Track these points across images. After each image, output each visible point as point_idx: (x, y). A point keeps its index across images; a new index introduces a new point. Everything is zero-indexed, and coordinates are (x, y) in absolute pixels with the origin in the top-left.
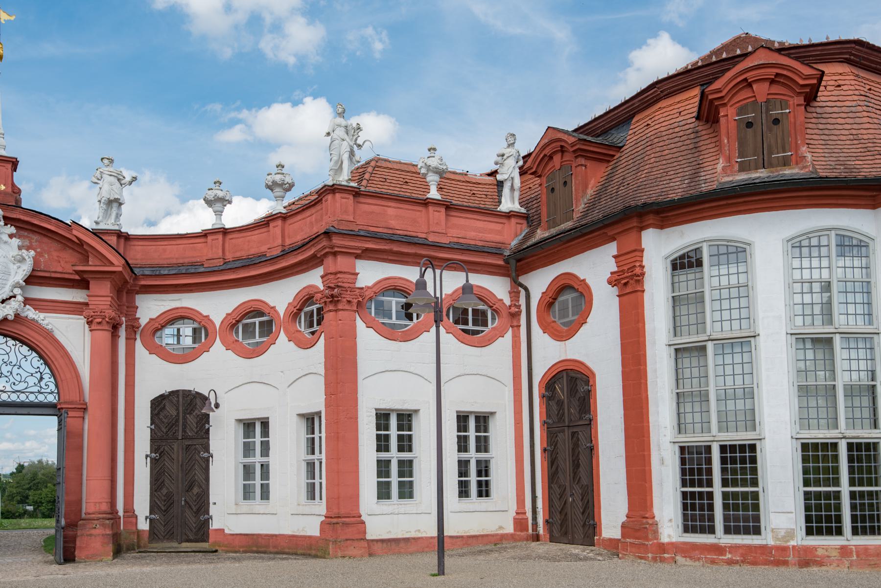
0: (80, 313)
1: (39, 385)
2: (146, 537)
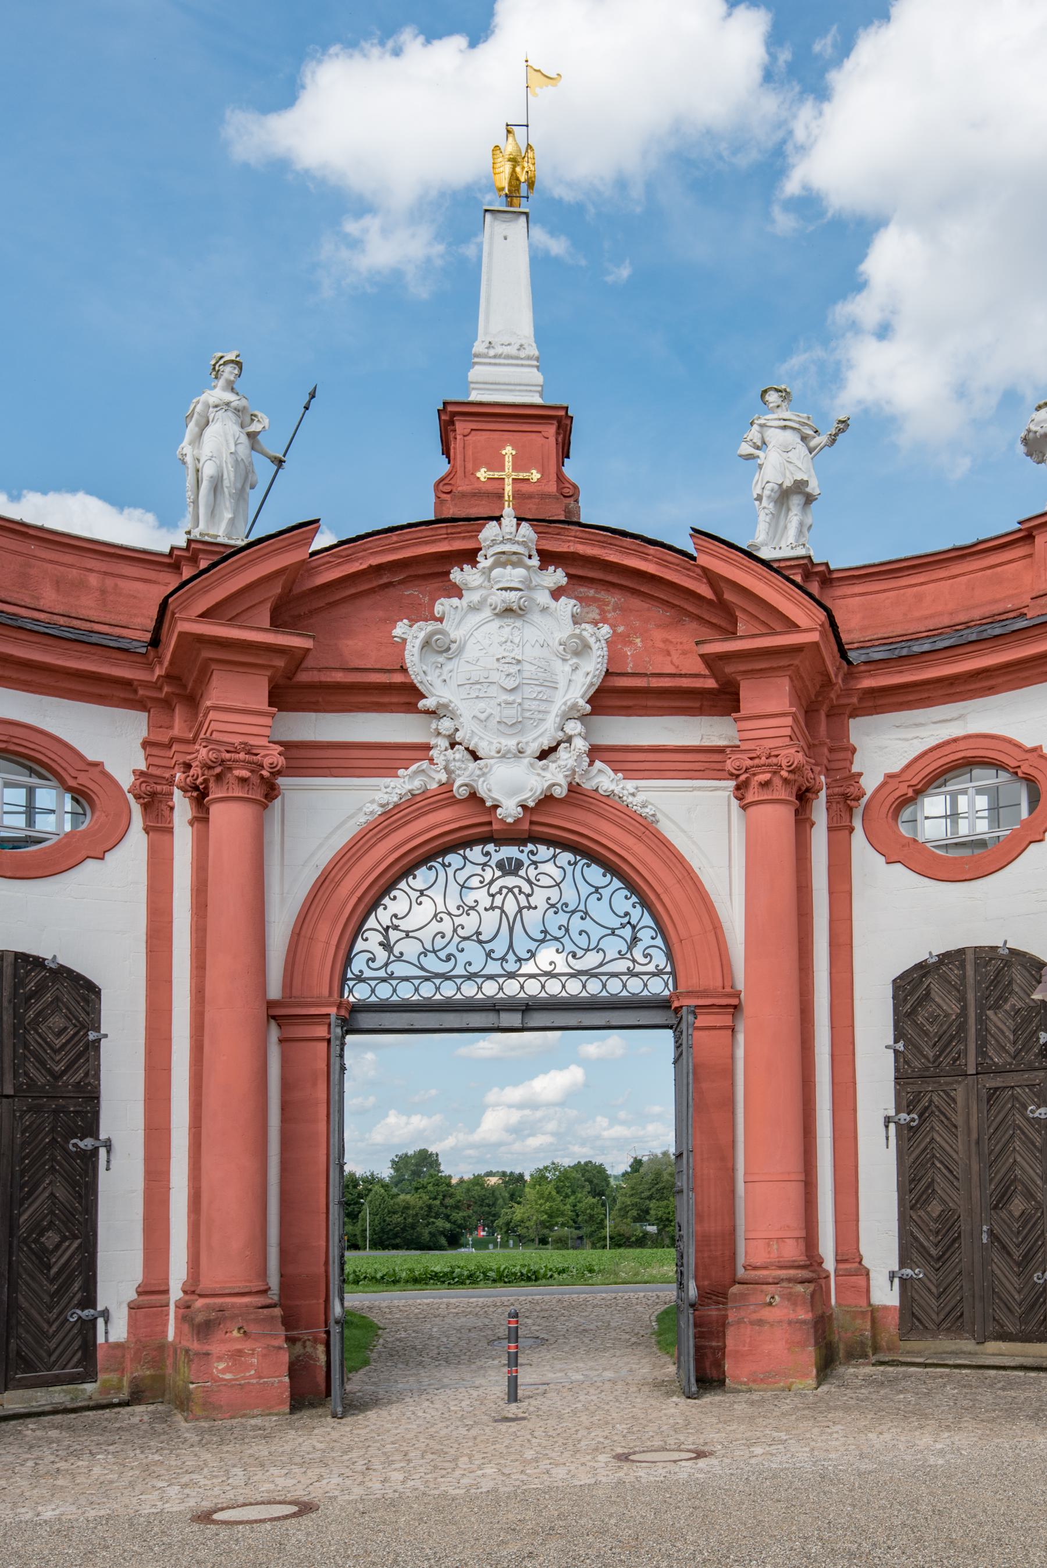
0: (717, 772)
1: (628, 956)
2: (892, 1324)
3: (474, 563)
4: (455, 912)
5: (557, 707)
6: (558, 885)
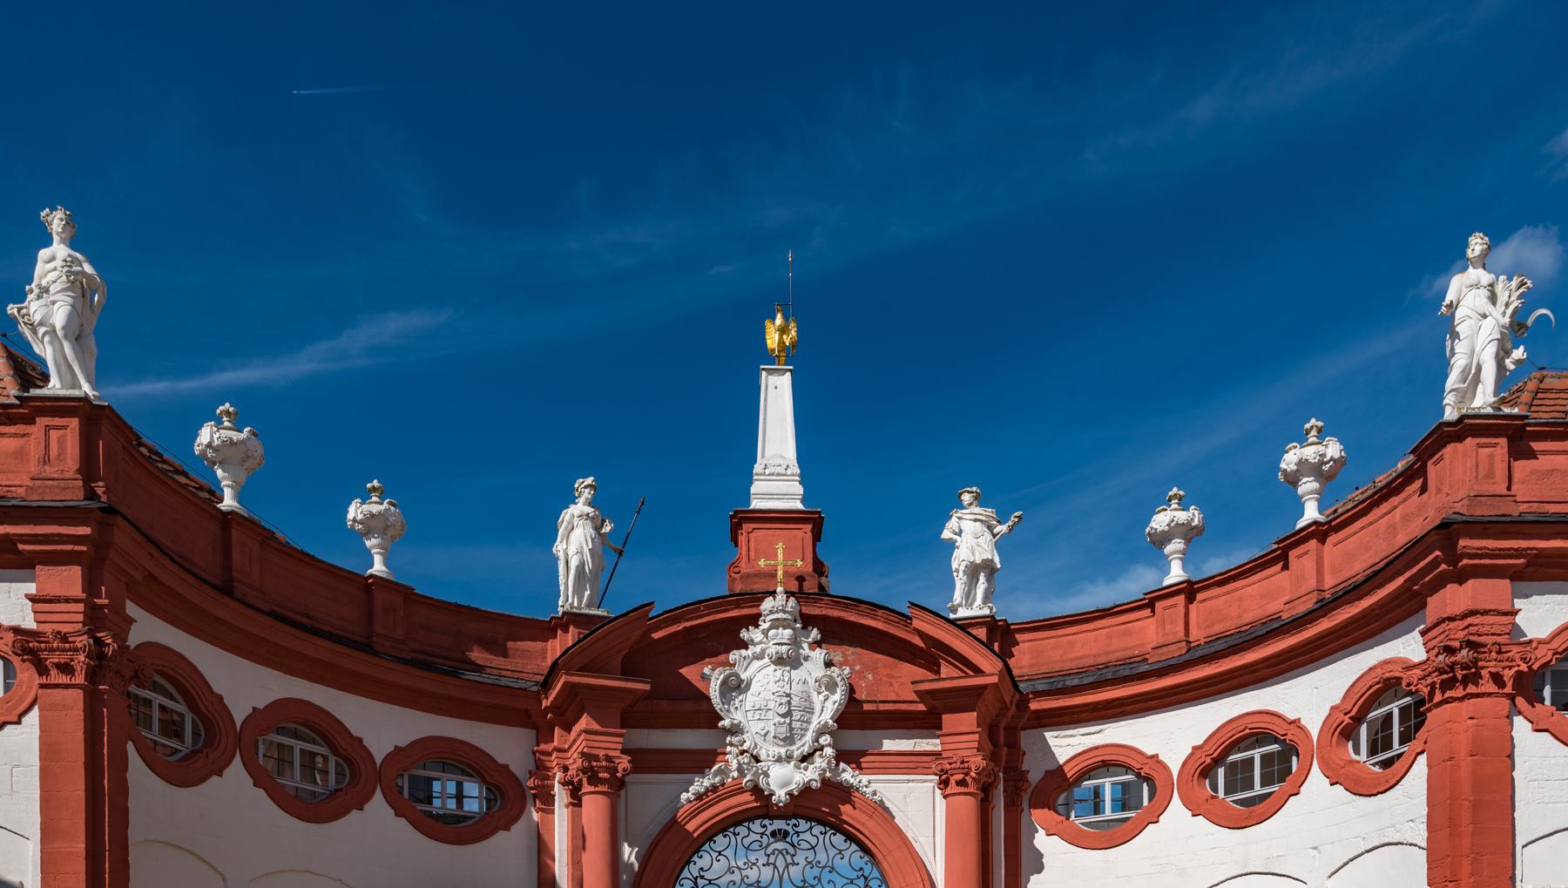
0: (925, 770)
3: (757, 626)
5: (813, 727)
6: (813, 848)
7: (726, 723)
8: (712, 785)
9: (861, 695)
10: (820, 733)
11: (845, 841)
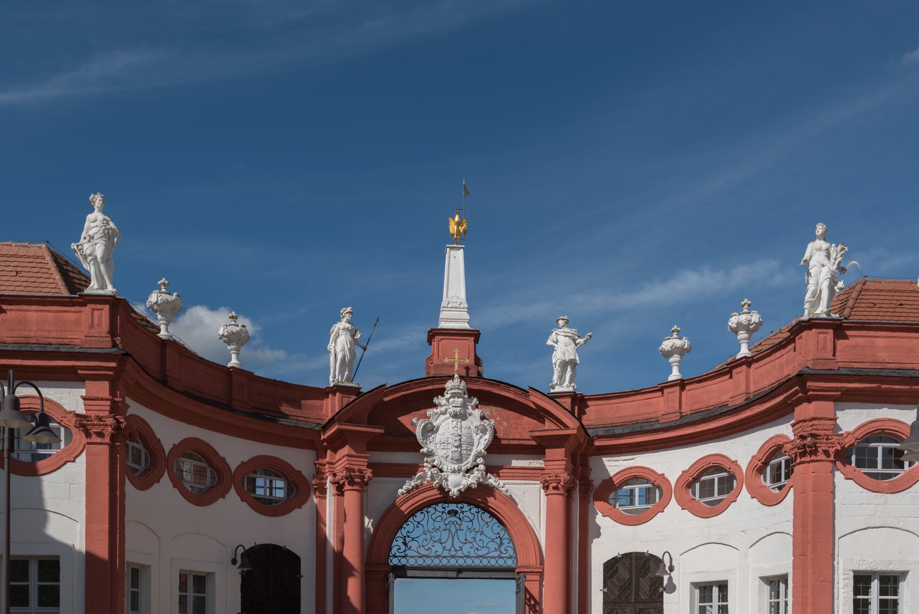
1: (499, 550)
3: (443, 396)
4: (431, 531)
5: (473, 453)
6: (471, 521)
7: (424, 450)
8: (416, 485)
9: (500, 435)
10: (477, 456)
11: (490, 517)
